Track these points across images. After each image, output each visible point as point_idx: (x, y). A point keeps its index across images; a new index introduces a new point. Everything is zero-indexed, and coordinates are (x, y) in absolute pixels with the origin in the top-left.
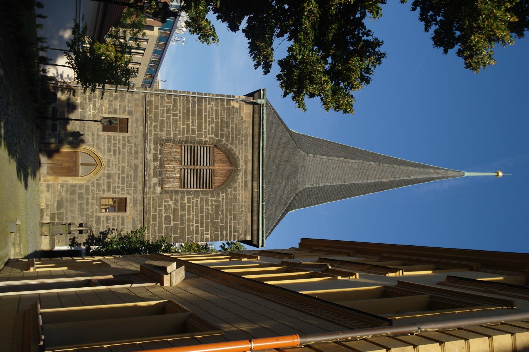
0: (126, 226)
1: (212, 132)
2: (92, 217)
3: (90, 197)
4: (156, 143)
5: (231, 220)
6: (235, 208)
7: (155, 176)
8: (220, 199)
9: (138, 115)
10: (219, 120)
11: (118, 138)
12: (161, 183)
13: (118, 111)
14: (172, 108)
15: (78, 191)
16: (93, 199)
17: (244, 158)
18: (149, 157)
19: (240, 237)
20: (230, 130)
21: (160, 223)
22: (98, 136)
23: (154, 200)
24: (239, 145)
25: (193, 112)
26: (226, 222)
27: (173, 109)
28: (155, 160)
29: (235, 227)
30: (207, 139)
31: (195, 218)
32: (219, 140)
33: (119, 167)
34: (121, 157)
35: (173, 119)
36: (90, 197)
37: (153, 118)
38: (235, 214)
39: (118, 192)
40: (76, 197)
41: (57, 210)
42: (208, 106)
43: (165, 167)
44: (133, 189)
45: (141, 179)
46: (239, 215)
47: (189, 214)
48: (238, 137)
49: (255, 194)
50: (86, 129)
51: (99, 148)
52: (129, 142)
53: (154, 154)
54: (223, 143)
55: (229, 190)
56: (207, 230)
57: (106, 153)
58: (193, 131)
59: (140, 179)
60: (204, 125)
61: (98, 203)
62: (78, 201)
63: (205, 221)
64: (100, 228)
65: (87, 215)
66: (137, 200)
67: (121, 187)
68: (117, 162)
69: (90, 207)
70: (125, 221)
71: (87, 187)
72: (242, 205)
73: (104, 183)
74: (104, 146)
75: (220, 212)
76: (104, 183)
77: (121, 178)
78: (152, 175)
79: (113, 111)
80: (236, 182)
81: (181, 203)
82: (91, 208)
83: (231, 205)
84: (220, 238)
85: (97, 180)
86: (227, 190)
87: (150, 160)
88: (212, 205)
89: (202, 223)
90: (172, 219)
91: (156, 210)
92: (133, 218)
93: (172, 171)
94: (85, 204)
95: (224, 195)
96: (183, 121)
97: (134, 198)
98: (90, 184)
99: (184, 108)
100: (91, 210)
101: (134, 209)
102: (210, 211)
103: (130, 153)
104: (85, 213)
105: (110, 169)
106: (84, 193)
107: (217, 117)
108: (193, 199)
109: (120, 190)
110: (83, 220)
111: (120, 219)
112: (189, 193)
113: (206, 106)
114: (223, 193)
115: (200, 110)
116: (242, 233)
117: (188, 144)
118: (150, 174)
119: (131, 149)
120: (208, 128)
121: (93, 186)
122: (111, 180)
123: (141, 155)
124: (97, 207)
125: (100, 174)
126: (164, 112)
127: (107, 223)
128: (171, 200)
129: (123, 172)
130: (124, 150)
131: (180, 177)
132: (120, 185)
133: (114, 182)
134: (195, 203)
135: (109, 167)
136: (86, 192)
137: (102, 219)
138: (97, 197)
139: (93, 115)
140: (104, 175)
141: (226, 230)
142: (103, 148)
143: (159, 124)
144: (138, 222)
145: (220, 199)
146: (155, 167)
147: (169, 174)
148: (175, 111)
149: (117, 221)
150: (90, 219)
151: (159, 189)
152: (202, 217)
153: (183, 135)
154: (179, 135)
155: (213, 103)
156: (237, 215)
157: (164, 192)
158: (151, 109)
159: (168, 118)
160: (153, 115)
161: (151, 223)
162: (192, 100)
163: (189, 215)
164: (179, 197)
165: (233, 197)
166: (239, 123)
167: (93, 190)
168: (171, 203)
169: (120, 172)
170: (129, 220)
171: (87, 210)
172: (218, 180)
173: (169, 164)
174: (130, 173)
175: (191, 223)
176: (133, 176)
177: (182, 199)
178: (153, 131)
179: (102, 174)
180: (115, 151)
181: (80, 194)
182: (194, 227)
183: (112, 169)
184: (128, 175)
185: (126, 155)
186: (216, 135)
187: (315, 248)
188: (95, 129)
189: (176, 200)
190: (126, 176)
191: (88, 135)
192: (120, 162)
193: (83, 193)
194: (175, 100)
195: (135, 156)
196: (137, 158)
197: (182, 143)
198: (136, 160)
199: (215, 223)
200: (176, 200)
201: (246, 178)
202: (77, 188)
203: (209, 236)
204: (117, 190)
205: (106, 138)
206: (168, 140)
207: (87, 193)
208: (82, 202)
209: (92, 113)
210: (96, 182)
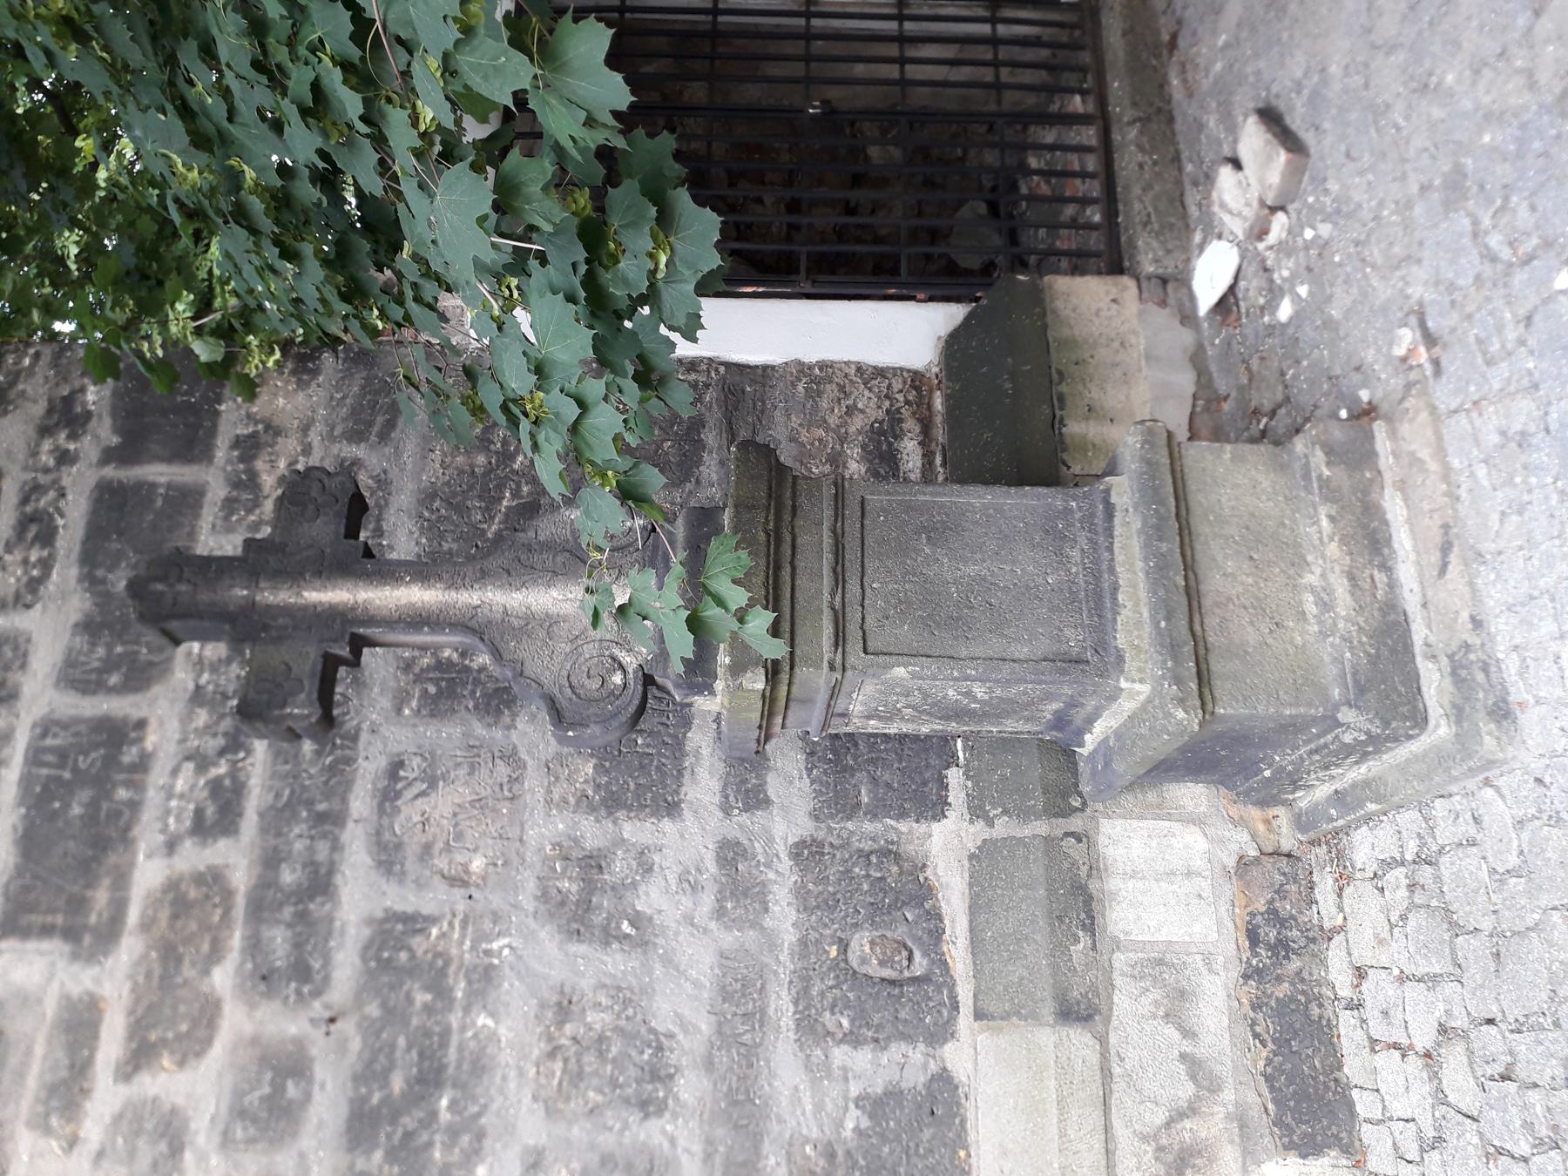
2: (194, 901)
41: (941, 1103)
64: (76, 677)
65: (298, 975)
110: (388, 857)
150: (236, 859)
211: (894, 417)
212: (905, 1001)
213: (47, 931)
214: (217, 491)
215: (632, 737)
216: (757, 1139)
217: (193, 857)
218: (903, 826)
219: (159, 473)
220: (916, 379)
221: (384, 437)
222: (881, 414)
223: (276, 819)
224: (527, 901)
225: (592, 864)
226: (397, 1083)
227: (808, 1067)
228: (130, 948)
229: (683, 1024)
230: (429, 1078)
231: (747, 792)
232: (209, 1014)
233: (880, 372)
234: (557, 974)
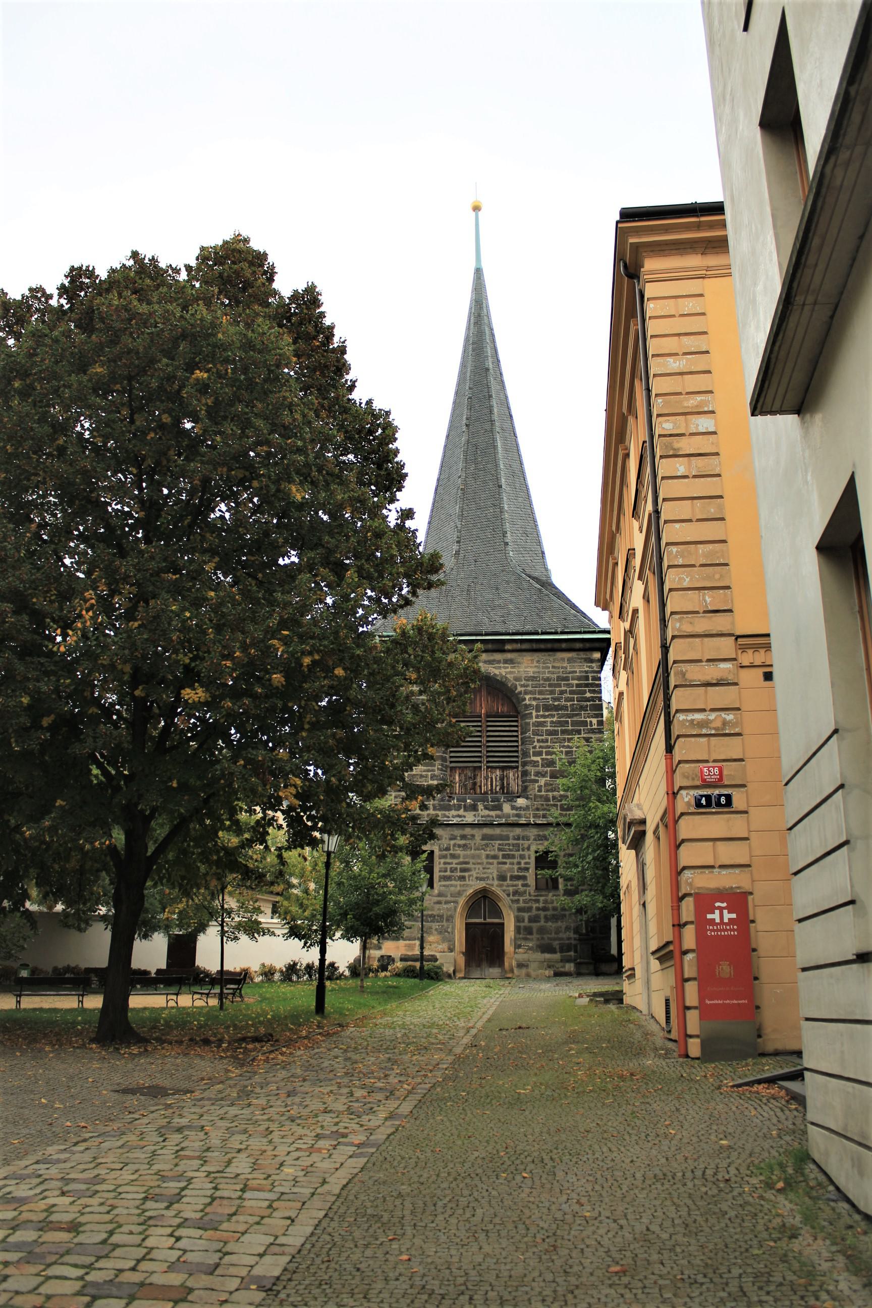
3: (535, 906)
4: (448, 808)
5: (568, 685)
6: (548, 679)
7: (499, 808)
8: (534, 703)
12: (511, 797)
15: (526, 923)
16: (537, 901)
18: (470, 818)
22: (440, 895)
23: (538, 809)
26: (572, 692)
28: (474, 808)
29: (579, 679)
34: (471, 861)
36: (535, 906)
38: (559, 678)
41: (555, 952)
43: (486, 793)
44: (521, 842)
45: (505, 829)
49: (525, 646)
51: (459, 894)
52: (448, 849)
53: (465, 810)
55: (519, 689)
56: (584, 723)
57: (467, 882)
59: (505, 831)
71: (520, 910)
78: (498, 812)
83: (543, 686)
85: (508, 895)
86: (520, 693)
88: (544, 716)
95: (527, 697)
103: (464, 847)
108: (535, 747)
109: (523, 862)
112: (526, 754)
118: (497, 816)
119: (459, 846)
121: (518, 901)
123: (468, 831)
128: (537, 781)
129: (495, 857)
132: (515, 861)
133: (511, 870)
140: (501, 886)
141: (585, 692)
145: (534, 703)
146: (486, 808)
151: (521, 802)
152: (563, 732)
157: (524, 793)
167: (524, 902)
168: (542, 781)
169: (495, 861)
171: (555, 909)
172: (502, 708)
177: (535, 764)
181: (530, 921)
184: (499, 850)
185: (468, 852)
187: (614, 528)
189: (537, 774)
196: (473, 836)
197: (446, 767)
199: (573, 710)
200: (537, 774)
201: (499, 662)
202: (522, 924)
203: (594, 721)
204: (523, 865)
207: (529, 909)
212: (561, 952)
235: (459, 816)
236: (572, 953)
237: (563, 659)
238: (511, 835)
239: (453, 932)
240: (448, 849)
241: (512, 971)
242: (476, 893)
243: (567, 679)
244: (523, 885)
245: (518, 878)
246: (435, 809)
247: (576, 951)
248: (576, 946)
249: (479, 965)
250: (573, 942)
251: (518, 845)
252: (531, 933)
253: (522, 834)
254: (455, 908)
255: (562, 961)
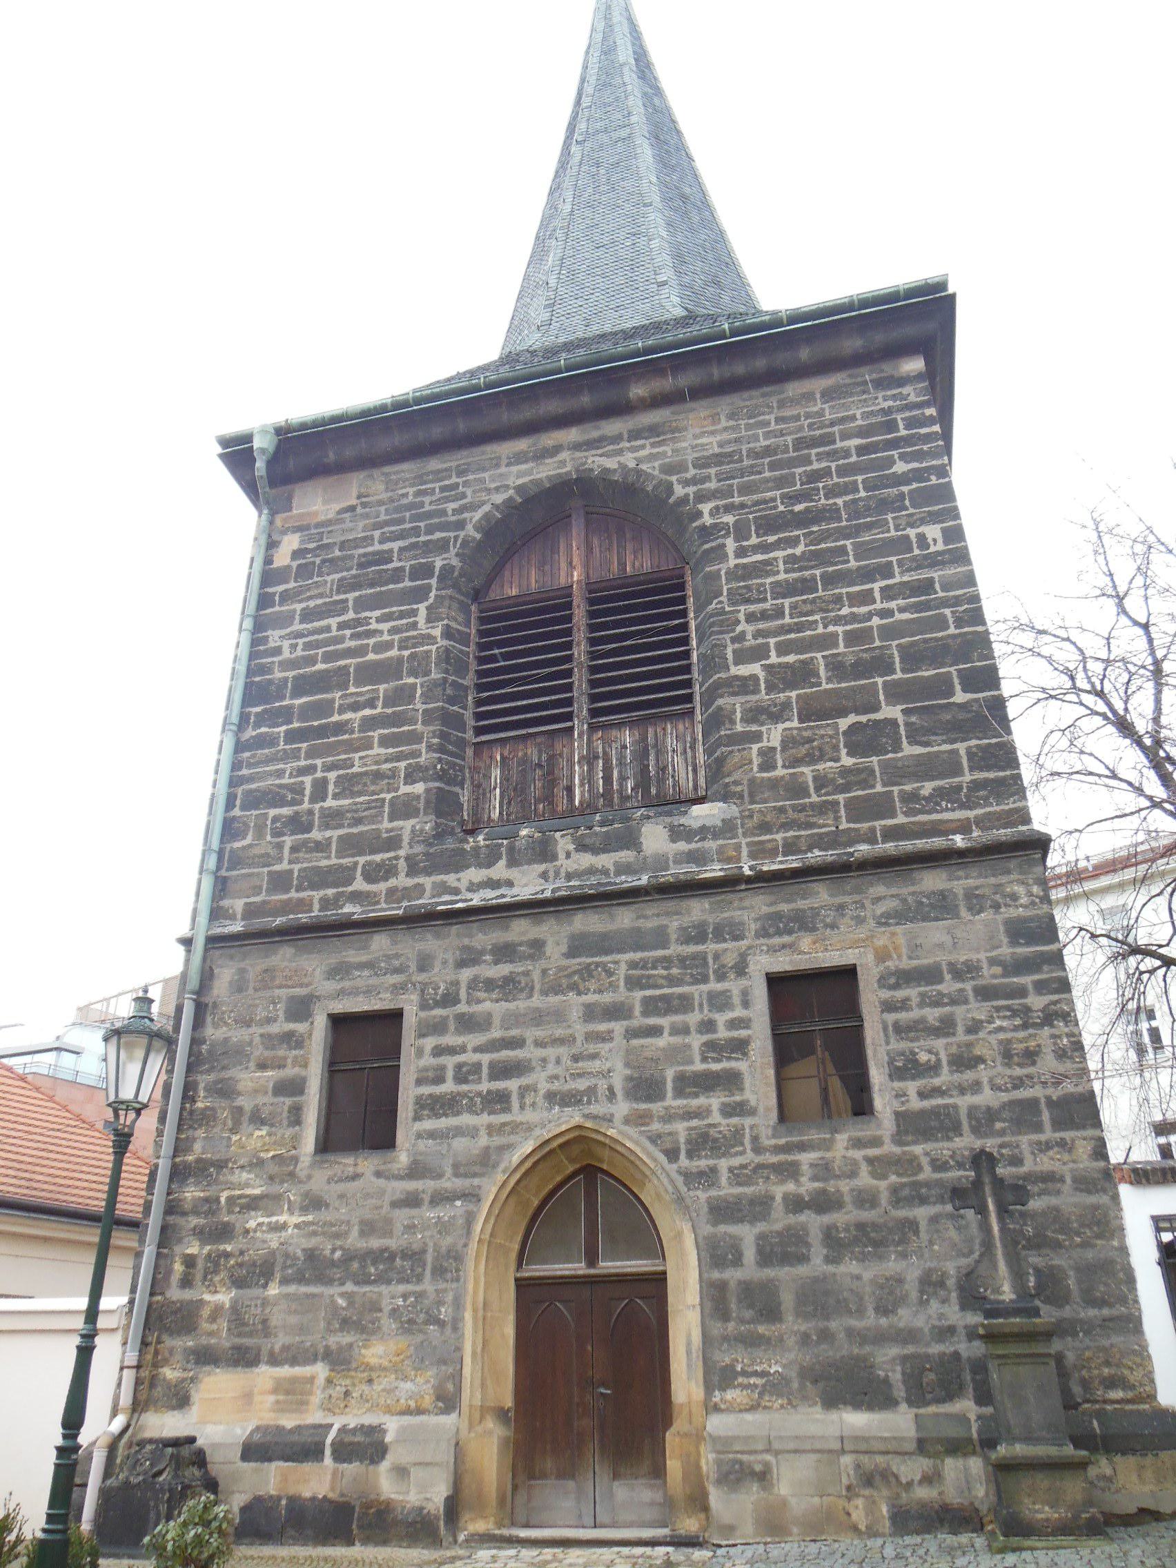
0: (943, 958)
1: (402, 615)
3: (779, 1191)
4: (456, 862)
6: (768, 451)
7: (630, 840)
8: (729, 519)
9: (311, 968)
10: (351, 596)
11: (428, 1061)
13: (290, 1072)
14: (286, 811)
15: (749, 1269)
16: (789, 1171)
17: (523, 467)
18: (528, 884)
19: (913, 398)
20: (395, 545)
21: (895, 774)
22: (416, 1170)
23: (765, 827)
24: (464, 496)
25: (305, 713)
27: (294, 803)
28: (543, 852)
29: (862, 432)
30: (437, 632)
31: (845, 611)
32: (441, 579)
33: (591, 1037)
34: (531, 1034)
35: (336, 796)
36: (779, 1191)
37: (330, 892)
39: (733, 1024)
40: (786, 1276)
42: (286, 654)
44: (711, 947)
45: (651, 909)
46: (801, 428)
47: (828, 641)
48: (427, 508)
50: (375, 1243)
51: (486, 1161)
52: (449, 999)
54: (455, 562)
55: (679, 491)
56: (903, 544)
57: (515, 1115)
58: (404, 695)
59: (649, 917)
60: (371, 656)
61: (814, 1135)
62: (817, 1264)
63: (853, 564)
64: (972, 1110)
66: (778, 916)
67: (707, 1014)
68: (563, 1051)
69: (845, 1186)
70: (906, 964)
71: (722, 1211)
72: (749, 427)
73: (689, 1115)
74: (473, 1132)
75: (799, 508)
76: (689, 1115)
77: (653, 1021)
78: (626, 856)
79: (288, 1101)
80: (639, 473)
81: (771, 688)
82: (853, 1174)
83: (752, 470)
84: (934, 480)
85: (672, 1154)
86: (684, 500)
87: (544, 876)
88: (764, 548)
89: (868, 575)
90: (863, 719)
91: (823, 808)
92: (884, 921)
93: (607, 770)
94: (826, 1219)
95: (706, 508)
96: (352, 747)
97: (763, 933)
98: (702, 1195)
99: (287, 756)
100: (865, 1179)
101: (833, 926)
102: (798, 551)
103: (508, 987)
104: (884, 1212)
105: (602, 1085)
106: (761, 1227)
107: (337, 608)
108: (741, 638)
110: (934, 1220)
111: (900, 994)
113: (286, 665)
114: (699, 514)
115: (303, 686)
116: (894, 398)
117: (468, 716)
118: (622, 869)
119: (490, 984)
120: (386, 637)
122: (670, 1074)
123: (521, 930)
124: (842, 1139)
125: (632, 1140)
126: (306, 842)
127: (934, 1069)
128: (757, 737)
129: (616, 1012)
130: (496, 1021)
131: (632, 724)
132: (693, 1018)
133: (677, 1054)
134: (761, 625)
135: (592, 1091)
136: (753, 1220)
137: (916, 1104)
138: (778, 1149)
139: (304, 1210)
140: (639, 1119)
141: (890, 462)
142: (483, 1140)
143: (362, 860)
144: (905, 891)
145: (729, 519)
146: (582, 847)
147: (623, 779)
148: (301, 792)
149: (915, 1014)
150: (927, 1174)
151: (704, 814)
153: (414, 738)
154: (416, 754)
155: (274, 637)
156: (806, 433)
157: (716, 784)
158: (286, 907)
159: (332, 818)
160: (317, 895)
161: (901, 819)
162: (257, 725)
163: (830, 640)
164: (736, 705)
165: (713, 471)
166: (367, 516)
167: (738, 1176)
168: (774, 735)
169: (618, 1027)
170: (901, 940)
171: (866, 1199)
172: (639, 562)
173: (570, 790)
174: (622, 970)
175: (876, 621)
176: (638, 955)
177: (746, 685)
178: (392, 882)
179: (632, 1131)
180: (502, 1071)
181: (766, 1257)
182: (893, 605)
183: (606, 1074)
184: (633, 983)
185: (520, 1005)
186: (419, 594)
188: (381, 1193)
190: (639, 995)
191: (410, 1228)
192: (559, 1032)
193: (761, 1237)
194: (255, 801)
195: (523, 958)
197: (462, 743)
198: (549, 950)
199: (855, 514)
201: (618, 438)
202: (733, 1275)
203: (933, 532)
204: (723, 1033)
205: (428, 1125)
206: (443, 804)
207: (759, 1208)
208: (815, 1237)
209: (296, 1219)
210: (684, 1161)
211: (1133, 1387)
213: (898, 1126)
214: (1043, 1137)
215: (971, 1297)
216: (873, 1343)
217: (925, 1161)
218: (971, 1390)
219: (1046, 1116)
220: (1152, 1397)
221: (1076, 1189)
222: (1132, 1381)
223: (939, 1183)
224: (928, 1264)
225: (941, 1284)
226: (872, 1235)
227: (894, 1359)
228: (897, 1150)
229: (900, 1319)
230: (877, 1244)
231: (972, 1335)
232: (884, 1177)
233: (1152, 1381)
234: (909, 1278)
235: (493, 884)
236: (966, 1406)
237: (809, 397)
238: (674, 924)
239: (456, 1324)
240: (449, 999)
241: (699, 1502)
242: (546, 1155)
243: (828, 440)
244: (730, 1110)
245: (707, 1082)
246: (412, 871)
247: (983, 1397)
248: (979, 1367)
249: (567, 1473)
250: (970, 1349)
251: (701, 959)
252: (771, 1313)
253: (711, 919)
254: (470, 1219)
255: (922, 1446)
